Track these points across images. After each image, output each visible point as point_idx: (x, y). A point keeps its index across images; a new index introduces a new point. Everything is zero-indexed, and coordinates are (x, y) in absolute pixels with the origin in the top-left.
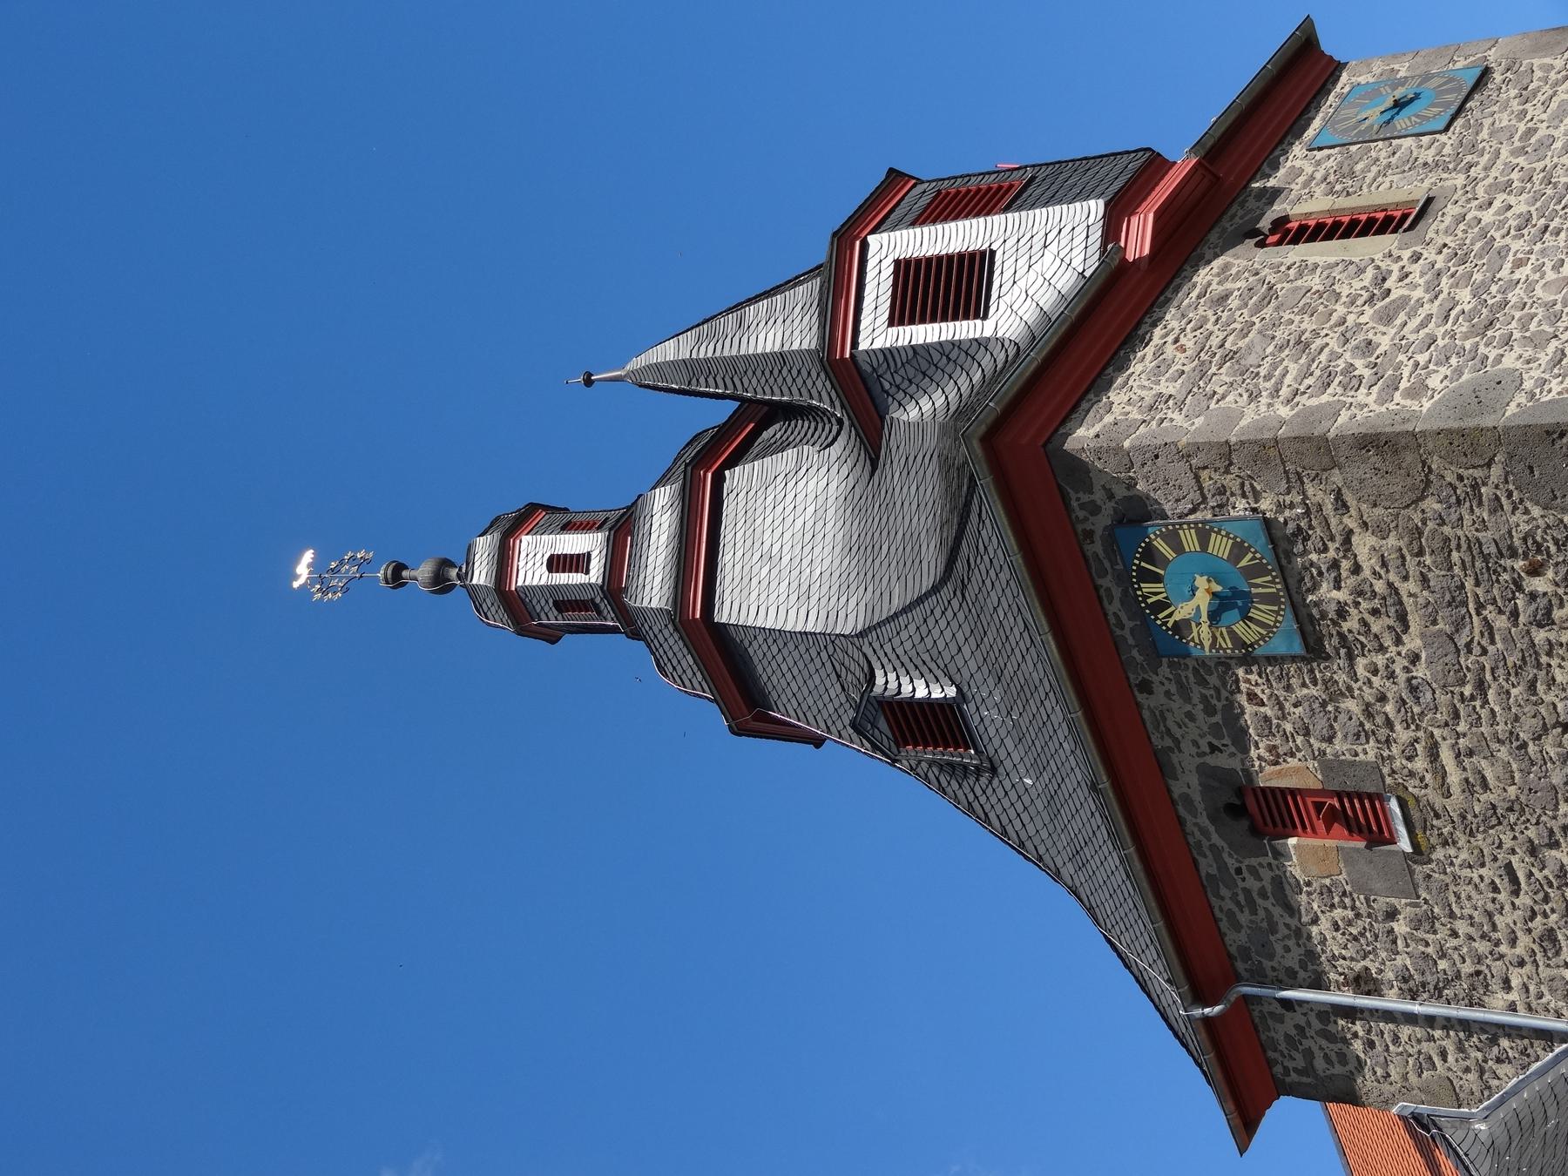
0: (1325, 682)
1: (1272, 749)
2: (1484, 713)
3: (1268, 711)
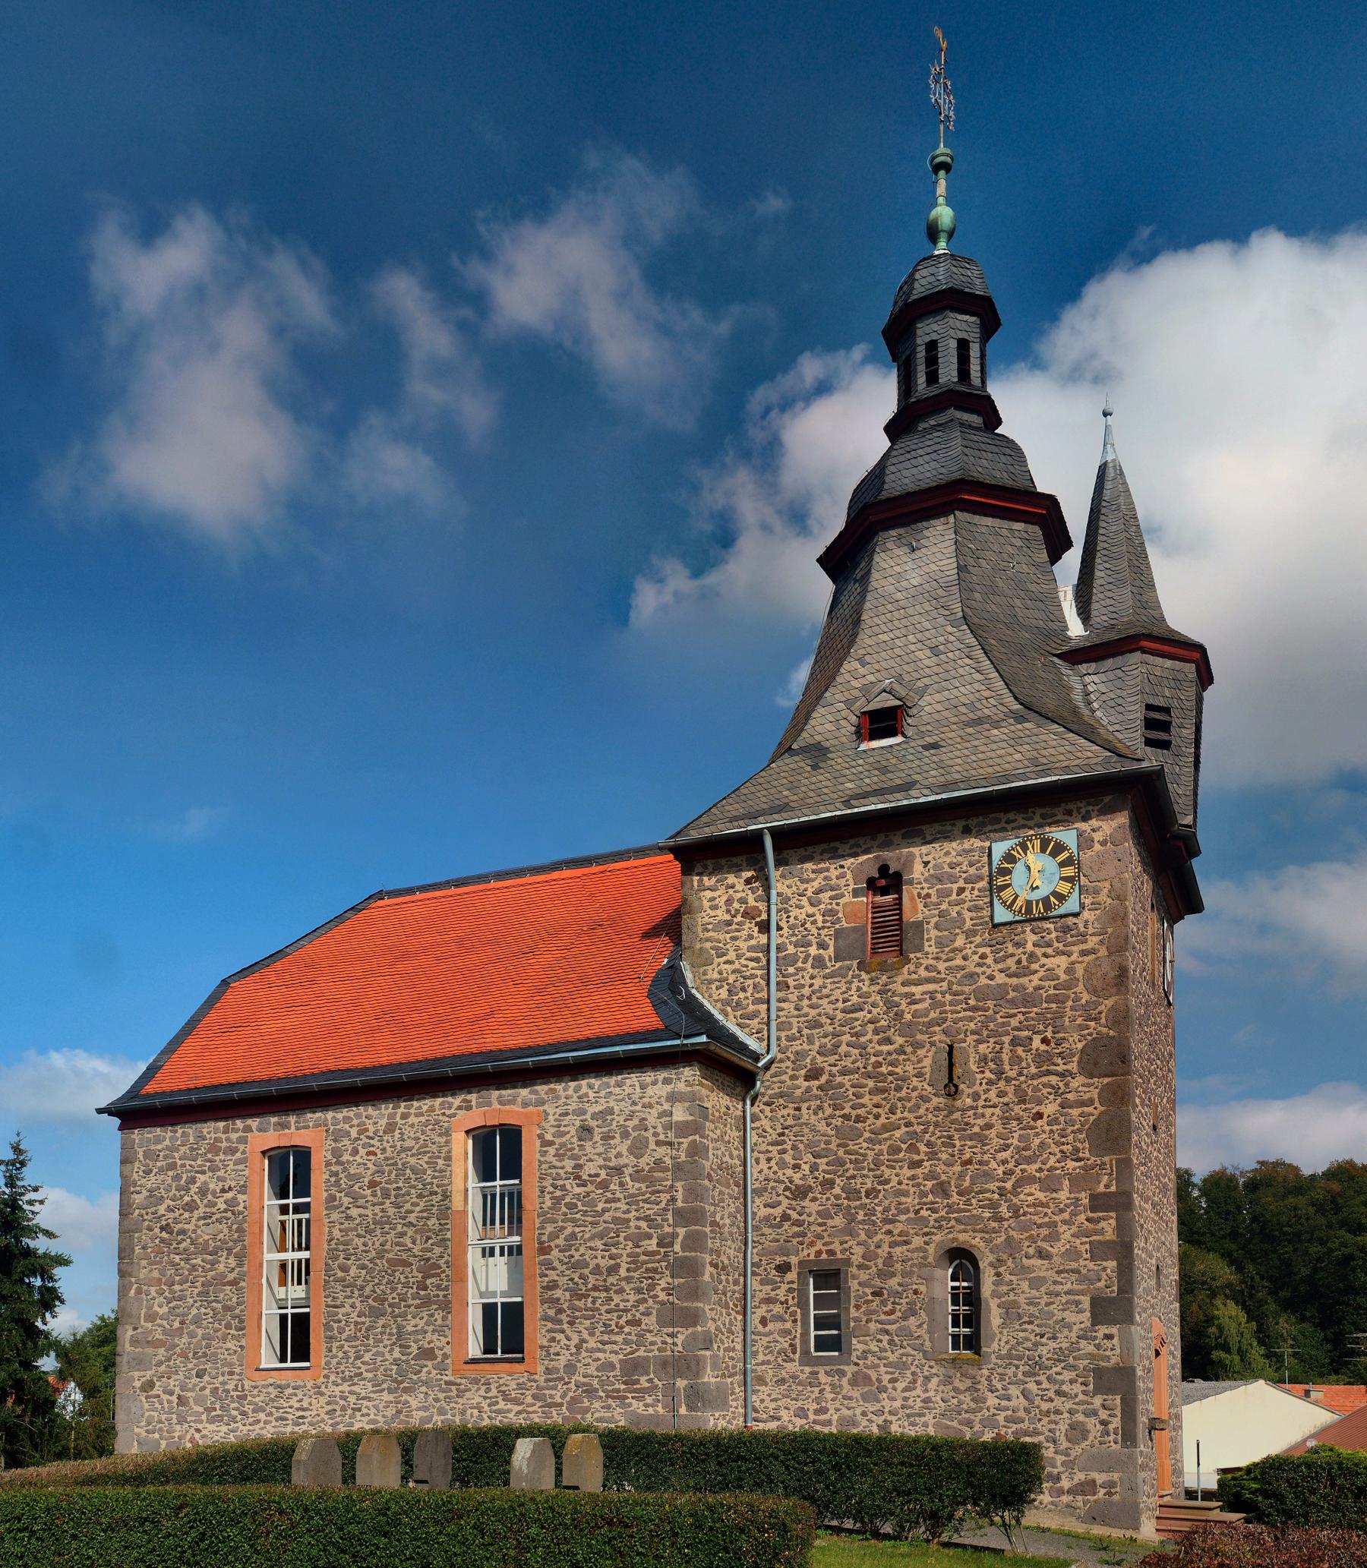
0: (974, 931)
1: (928, 896)
2: (958, 1008)
3: (954, 896)
